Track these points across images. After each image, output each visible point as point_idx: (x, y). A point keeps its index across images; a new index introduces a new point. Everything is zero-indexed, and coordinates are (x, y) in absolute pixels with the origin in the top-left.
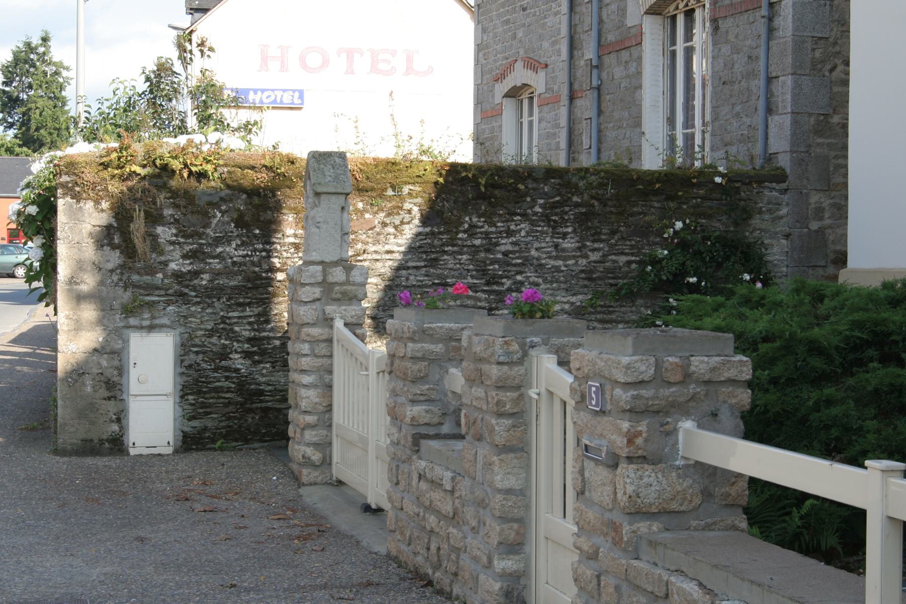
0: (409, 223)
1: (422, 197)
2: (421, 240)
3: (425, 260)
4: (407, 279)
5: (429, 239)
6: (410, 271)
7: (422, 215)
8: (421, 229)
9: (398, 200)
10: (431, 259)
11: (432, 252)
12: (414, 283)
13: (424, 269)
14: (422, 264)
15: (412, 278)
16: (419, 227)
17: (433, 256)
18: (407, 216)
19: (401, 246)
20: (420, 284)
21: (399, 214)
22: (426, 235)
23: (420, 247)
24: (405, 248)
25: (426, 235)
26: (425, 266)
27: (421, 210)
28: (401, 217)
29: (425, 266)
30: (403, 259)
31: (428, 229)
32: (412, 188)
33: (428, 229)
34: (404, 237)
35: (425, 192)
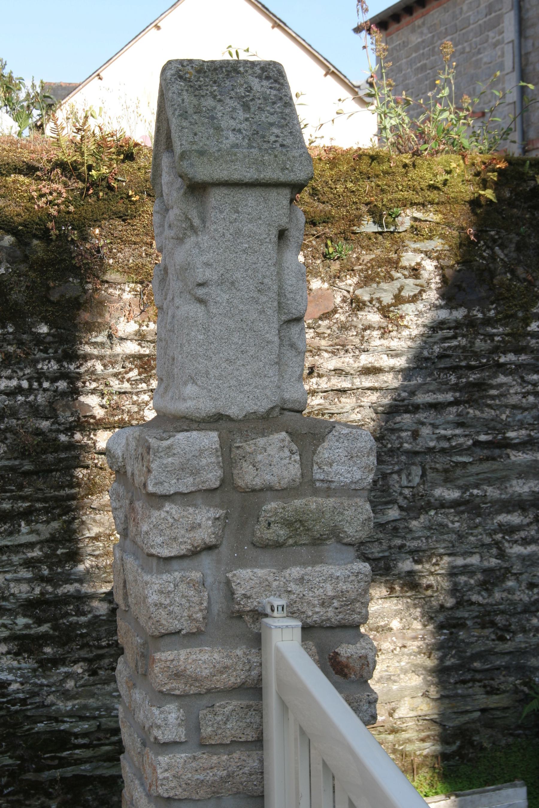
0: (414, 299)
1: (443, 236)
2: (445, 339)
3: (455, 388)
4: (415, 435)
5: (463, 336)
6: (421, 416)
7: (444, 280)
8: (443, 314)
9: (388, 244)
10: (470, 385)
11: (470, 368)
12: (432, 444)
13: (453, 410)
14: (449, 397)
15: (425, 431)
16: (438, 307)
17: (473, 377)
18: (411, 281)
19: (397, 356)
20: (446, 445)
21: (392, 279)
22: (456, 328)
23: (441, 357)
24: (408, 361)
25: (456, 328)
26: (456, 403)
27: (440, 268)
28: (397, 284)
29: (456, 403)
30: (403, 388)
31: (459, 314)
32: (418, 215)
33: (459, 314)
34: (405, 333)
35: (449, 225)
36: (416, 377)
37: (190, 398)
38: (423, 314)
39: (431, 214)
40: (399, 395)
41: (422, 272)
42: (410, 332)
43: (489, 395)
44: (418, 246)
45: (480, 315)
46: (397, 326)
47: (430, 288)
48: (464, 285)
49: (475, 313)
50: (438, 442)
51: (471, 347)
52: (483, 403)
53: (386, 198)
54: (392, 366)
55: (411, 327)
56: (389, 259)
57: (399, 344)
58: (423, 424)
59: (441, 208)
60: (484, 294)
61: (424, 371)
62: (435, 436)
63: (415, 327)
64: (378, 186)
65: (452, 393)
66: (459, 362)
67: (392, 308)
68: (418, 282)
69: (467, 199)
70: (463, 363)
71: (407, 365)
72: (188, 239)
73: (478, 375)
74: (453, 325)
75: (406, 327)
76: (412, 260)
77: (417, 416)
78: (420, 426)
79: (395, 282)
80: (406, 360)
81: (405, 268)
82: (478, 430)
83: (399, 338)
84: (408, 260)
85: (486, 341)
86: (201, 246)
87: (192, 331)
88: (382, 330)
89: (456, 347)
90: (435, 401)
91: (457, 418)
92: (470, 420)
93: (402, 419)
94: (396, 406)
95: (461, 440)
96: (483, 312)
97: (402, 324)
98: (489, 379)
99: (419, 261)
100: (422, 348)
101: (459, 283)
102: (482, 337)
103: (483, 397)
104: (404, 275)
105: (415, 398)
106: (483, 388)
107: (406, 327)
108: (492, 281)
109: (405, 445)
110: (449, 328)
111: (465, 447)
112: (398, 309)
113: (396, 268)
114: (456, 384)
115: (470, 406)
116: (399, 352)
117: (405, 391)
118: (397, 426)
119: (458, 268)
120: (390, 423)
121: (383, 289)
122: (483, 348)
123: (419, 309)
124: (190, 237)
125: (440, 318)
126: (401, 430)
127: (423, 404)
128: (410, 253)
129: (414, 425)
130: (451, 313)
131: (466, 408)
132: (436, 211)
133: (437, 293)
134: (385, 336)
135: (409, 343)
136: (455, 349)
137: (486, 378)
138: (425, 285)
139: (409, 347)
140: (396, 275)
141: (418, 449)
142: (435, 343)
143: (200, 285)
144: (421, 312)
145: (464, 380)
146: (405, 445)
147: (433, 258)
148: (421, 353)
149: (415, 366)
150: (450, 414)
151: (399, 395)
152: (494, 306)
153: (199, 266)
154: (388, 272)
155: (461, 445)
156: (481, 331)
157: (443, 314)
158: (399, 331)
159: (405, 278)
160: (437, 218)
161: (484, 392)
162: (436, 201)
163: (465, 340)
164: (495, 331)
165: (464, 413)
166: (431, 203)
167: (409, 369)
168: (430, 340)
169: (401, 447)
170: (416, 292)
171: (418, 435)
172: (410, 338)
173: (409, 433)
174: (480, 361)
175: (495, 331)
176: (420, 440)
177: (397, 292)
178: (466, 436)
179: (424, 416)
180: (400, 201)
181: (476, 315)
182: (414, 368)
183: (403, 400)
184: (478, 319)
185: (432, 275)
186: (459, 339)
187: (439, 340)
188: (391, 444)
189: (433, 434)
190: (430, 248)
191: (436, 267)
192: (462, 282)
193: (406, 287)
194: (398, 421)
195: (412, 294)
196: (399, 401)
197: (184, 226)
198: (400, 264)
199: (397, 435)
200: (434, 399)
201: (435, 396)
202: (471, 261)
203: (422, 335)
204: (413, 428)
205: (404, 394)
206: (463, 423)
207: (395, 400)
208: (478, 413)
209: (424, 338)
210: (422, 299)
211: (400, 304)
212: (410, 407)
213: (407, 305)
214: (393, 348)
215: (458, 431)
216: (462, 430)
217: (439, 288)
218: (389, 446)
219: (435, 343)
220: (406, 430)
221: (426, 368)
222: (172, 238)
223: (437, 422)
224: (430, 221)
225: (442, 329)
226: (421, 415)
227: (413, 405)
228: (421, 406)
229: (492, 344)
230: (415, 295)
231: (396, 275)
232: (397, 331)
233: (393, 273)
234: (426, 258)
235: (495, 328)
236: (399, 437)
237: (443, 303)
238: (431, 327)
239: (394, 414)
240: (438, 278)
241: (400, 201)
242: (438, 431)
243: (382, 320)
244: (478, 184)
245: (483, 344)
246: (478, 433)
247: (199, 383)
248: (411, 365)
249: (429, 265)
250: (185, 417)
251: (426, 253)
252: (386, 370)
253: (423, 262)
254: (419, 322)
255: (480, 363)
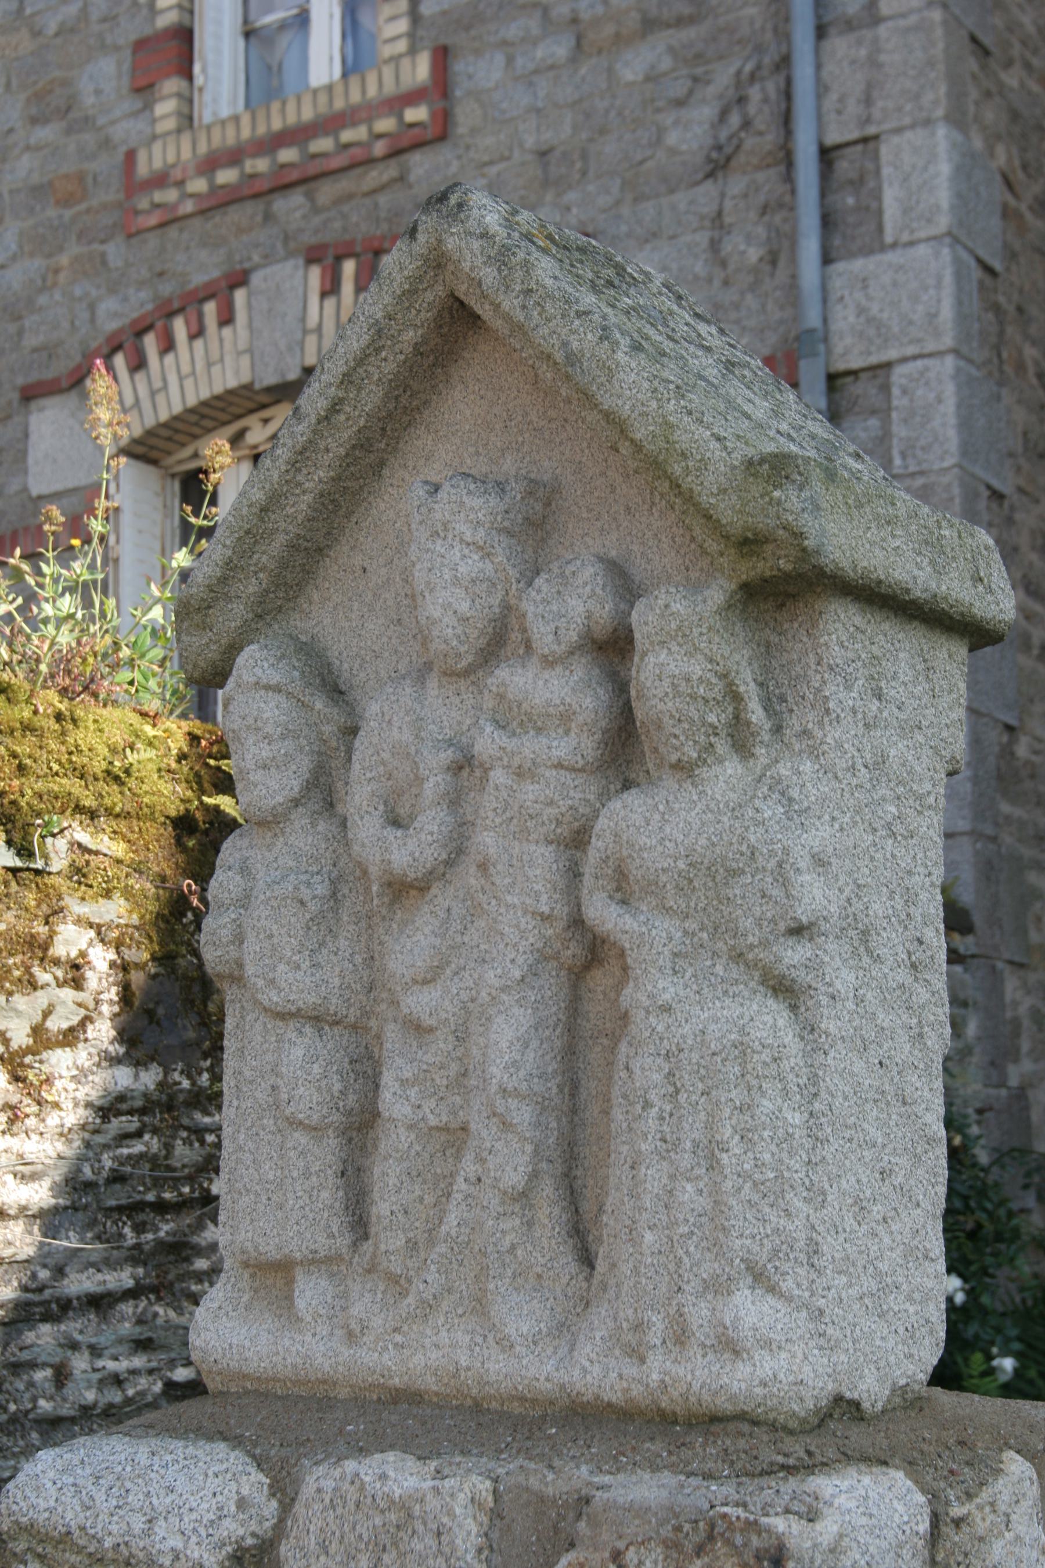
0: (70, 1037)
1: (128, 893)
2: (125, 1137)
3: (136, 1256)
4: (61, 1375)
5: (155, 1131)
6: (72, 1327)
7: (126, 996)
8: (124, 1077)
9: (30, 898)
10: (161, 1246)
11: (161, 1208)
12: (90, 1396)
13: (127, 1308)
14: (123, 1278)
15: (80, 1363)
16: (114, 1061)
17: (165, 1228)
18: (68, 994)
19: (34, 1177)
20: (115, 1396)
21: (34, 985)
22: (143, 1111)
23: (117, 1178)
24: (56, 1189)
25: (143, 1111)
26: (132, 1294)
27: (123, 967)
28: (42, 999)
29: (132, 1294)
30: (43, 1256)
31: (150, 1078)
32: (83, 837)
33: (150, 1078)
34: (53, 1119)
35: (138, 869)
36: (68, 1230)
37: (767, 1344)
38: (86, 1076)
39: (106, 838)
40: (34, 1276)
41: (89, 974)
42: (61, 1118)
43: (194, 1271)
44: (87, 910)
45: (186, 1084)
46: (39, 1103)
47: (100, 1013)
48: (161, 1011)
49: (176, 1076)
50: (100, 1390)
51: (166, 1158)
52: (182, 1290)
53: (31, 786)
54: (23, 1202)
55: (64, 1106)
56: (32, 936)
57: (41, 1147)
58: (74, 1346)
59: (123, 826)
60: (191, 1034)
61: (80, 1215)
62: (97, 1376)
63: (71, 1105)
64: (14, 755)
65: (130, 1269)
66: (144, 1193)
67: (28, 1059)
68: (81, 996)
69: (173, 813)
70: (150, 1197)
71: (53, 1201)
72: (717, 769)
73: (172, 1224)
74: (139, 1103)
75: (56, 1105)
76: (74, 944)
77: (63, 1327)
78: (69, 1353)
79: (40, 993)
80: (51, 1189)
81: (57, 962)
82: (173, 1355)
83: (41, 1134)
84: (67, 942)
85: (191, 1144)
86: (795, 793)
87: (763, 1094)
88: (10, 1113)
89: (142, 1156)
90: (99, 1289)
91: (138, 1329)
92: (162, 1333)
93: (38, 1337)
94: (28, 1304)
95: (143, 1382)
96: (189, 1077)
97: (50, 1098)
98: (193, 1233)
99: (84, 947)
100: (81, 1159)
101: (151, 1006)
102: (185, 1134)
103: (181, 1278)
104: (56, 978)
105: (66, 1282)
106: (184, 1254)
107: (56, 1105)
108: (206, 1006)
109: (42, 1402)
110: (130, 1112)
111: (150, 1398)
112: (41, 1062)
113: (42, 960)
114: (137, 1246)
115: (159, 1299)
116: (40, 1167)
117: (45, 1266)
118: (25, 1356)
119: (153, 971)
120: (13, 1348)
121: (16, 1010)
122: (186, 1160)
123: (79, 1063)
124: (721, 761)
125: (119, 1088)
126: (33, 1365)
127: (78, 1298)
128: (71, 927)
129: (59, 1350)
130: (136, 1076)
131: (151, 1304)
132: (115, 832)
133: (113, 1027)
134: (15, 1128)
135: (60, 1146)
136: (138, 1162)
137: (187, 1230)
138: (92, 1005)
139: (60, 1157)
140: (43, 977)
141: (66, 1411)
142: (106, 1147)
143: (798, 931)
144: (81, 1070)
145: (150, 1236)
146: (42, 1402)
147: (110, 942)
148: (79, 1170)
149: (68, 1203)
150: (123, 1319)
151: (34, 1276)
152: (208, 1062)
153: (802, 865)
154: (28, 969)
155: (142, 1394)
156: (185, 1121)
157: (124, 1077)
158: (42, 1115)
159: (58, 986)
160: (118, 849)
161: (185, 1265)
162: (118, 809)
163: (155, 1140)
164: (207, 1120)
165: (149, 1316)
166: (109, 812)
167: (55, 1210)
168: (99, 1139)
169: (35, 1407)
170: (75, 1020)
171: (68, 1376)
172: (61, 1135)
173: (49, 1372)
174: (178, 1190)
175: (207, 1120)
176: (69, 1390)
177: (40, 1018)
178: (151, 1372)
179: (78, 1326)
180: (56, 798)
181: (180, 1083)
182: (66, 1208)
183: (40, 1290)
184: (181, 1091)
185: (105, 984)
186: (147, 1137)
187: (114, 1139)
188: (15, 1402)
189: (95, 1370)
190: (107, 918)
191: (112, 965)
192: (157, 1003)
193: (58, 1008)
194: (29, 1341)
195: (65, 1025)
196: (33, 1291)
197: (712, 718)
198: (51, 952)
199: (25, 1377)
200: (99, 1283)
201: (100, 1277)
202: (174, 958)
203: (83, 1127)
204: (57, 1359)
205: (44, 1274)
206: (150, 1340)
207: (25, 1289)
208: (172, 1314)
209: (87, 1135)
210: (86, 1040)
211: (47, 1048)
212: (54, 1306)
213: (59, 1051)
214: (30, 1157)
215: (139, 1361)
216: (145, 1358)
217: (116, 1015)
218: (12, 1407)
219: (106, 1147)
220: (45, 1365)
221: (86, 1207)
222: (559, 766)
223: (102, 1340)
224: (105, 855)
225: (119, 1113)
226: (72, 1324)
227: (58, 1301)
228: (75, 1302)
229: (203, 1152)
230: (71, 1029)
231: (43, 977)
232: (37, 1115)
233: (36, 970)
234: (96, 942)
235: (209, 1114)
236: (31, 1384)
237: (122, 1050)
238: (101, 1109)
239: (20, 1325)
240: (114, 990)
241: (56, 798)
242: (100, 1363)
243: (11, 1088)
244: (187, 781)
245: (187, 1151)
246: (172, 1364)
247: (788, 1285)
248: (61, 1201)
249: (101, 958)
250: (741, 1416)
251: (98, 928)
252: (12, 1212)
253: (91, 951)
254: (80, 1095)
255: (180, 1194)
